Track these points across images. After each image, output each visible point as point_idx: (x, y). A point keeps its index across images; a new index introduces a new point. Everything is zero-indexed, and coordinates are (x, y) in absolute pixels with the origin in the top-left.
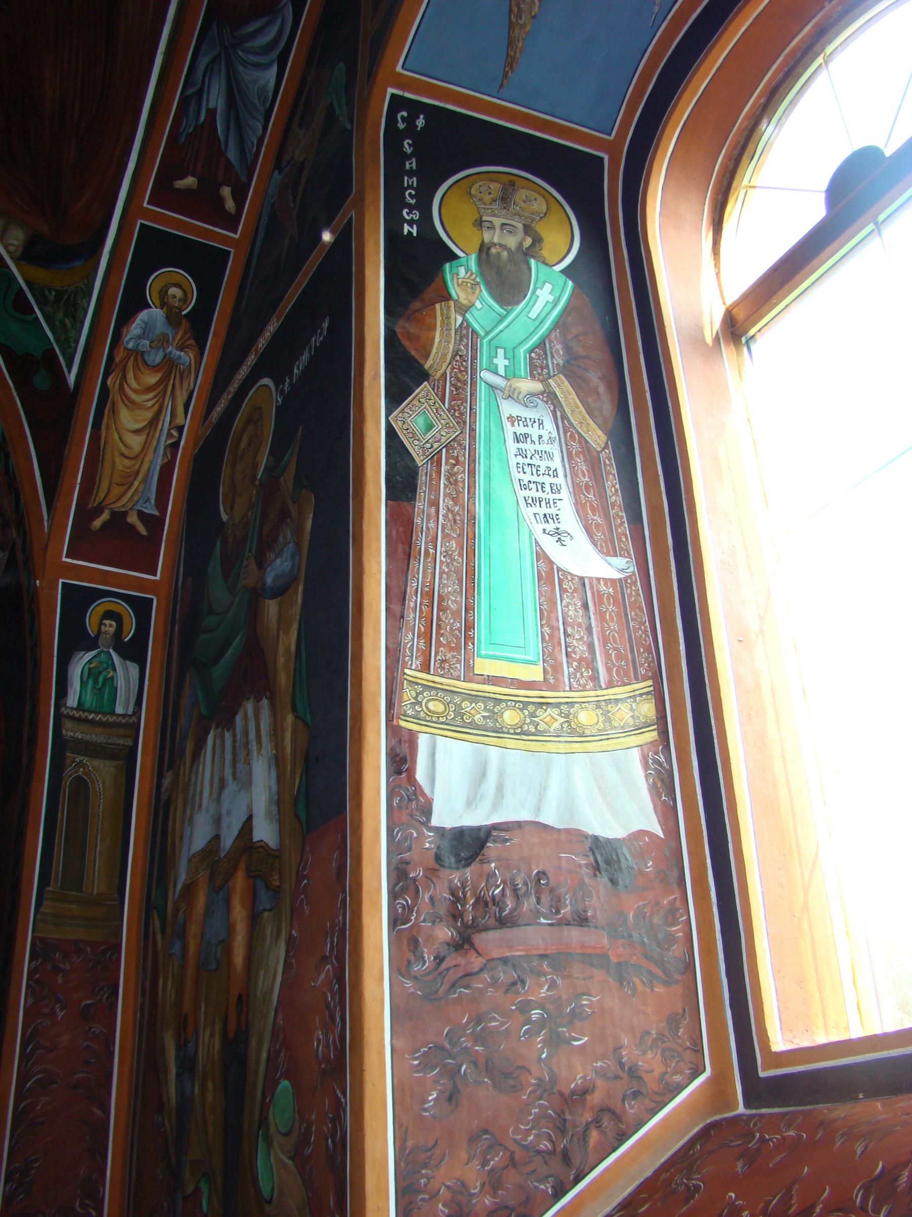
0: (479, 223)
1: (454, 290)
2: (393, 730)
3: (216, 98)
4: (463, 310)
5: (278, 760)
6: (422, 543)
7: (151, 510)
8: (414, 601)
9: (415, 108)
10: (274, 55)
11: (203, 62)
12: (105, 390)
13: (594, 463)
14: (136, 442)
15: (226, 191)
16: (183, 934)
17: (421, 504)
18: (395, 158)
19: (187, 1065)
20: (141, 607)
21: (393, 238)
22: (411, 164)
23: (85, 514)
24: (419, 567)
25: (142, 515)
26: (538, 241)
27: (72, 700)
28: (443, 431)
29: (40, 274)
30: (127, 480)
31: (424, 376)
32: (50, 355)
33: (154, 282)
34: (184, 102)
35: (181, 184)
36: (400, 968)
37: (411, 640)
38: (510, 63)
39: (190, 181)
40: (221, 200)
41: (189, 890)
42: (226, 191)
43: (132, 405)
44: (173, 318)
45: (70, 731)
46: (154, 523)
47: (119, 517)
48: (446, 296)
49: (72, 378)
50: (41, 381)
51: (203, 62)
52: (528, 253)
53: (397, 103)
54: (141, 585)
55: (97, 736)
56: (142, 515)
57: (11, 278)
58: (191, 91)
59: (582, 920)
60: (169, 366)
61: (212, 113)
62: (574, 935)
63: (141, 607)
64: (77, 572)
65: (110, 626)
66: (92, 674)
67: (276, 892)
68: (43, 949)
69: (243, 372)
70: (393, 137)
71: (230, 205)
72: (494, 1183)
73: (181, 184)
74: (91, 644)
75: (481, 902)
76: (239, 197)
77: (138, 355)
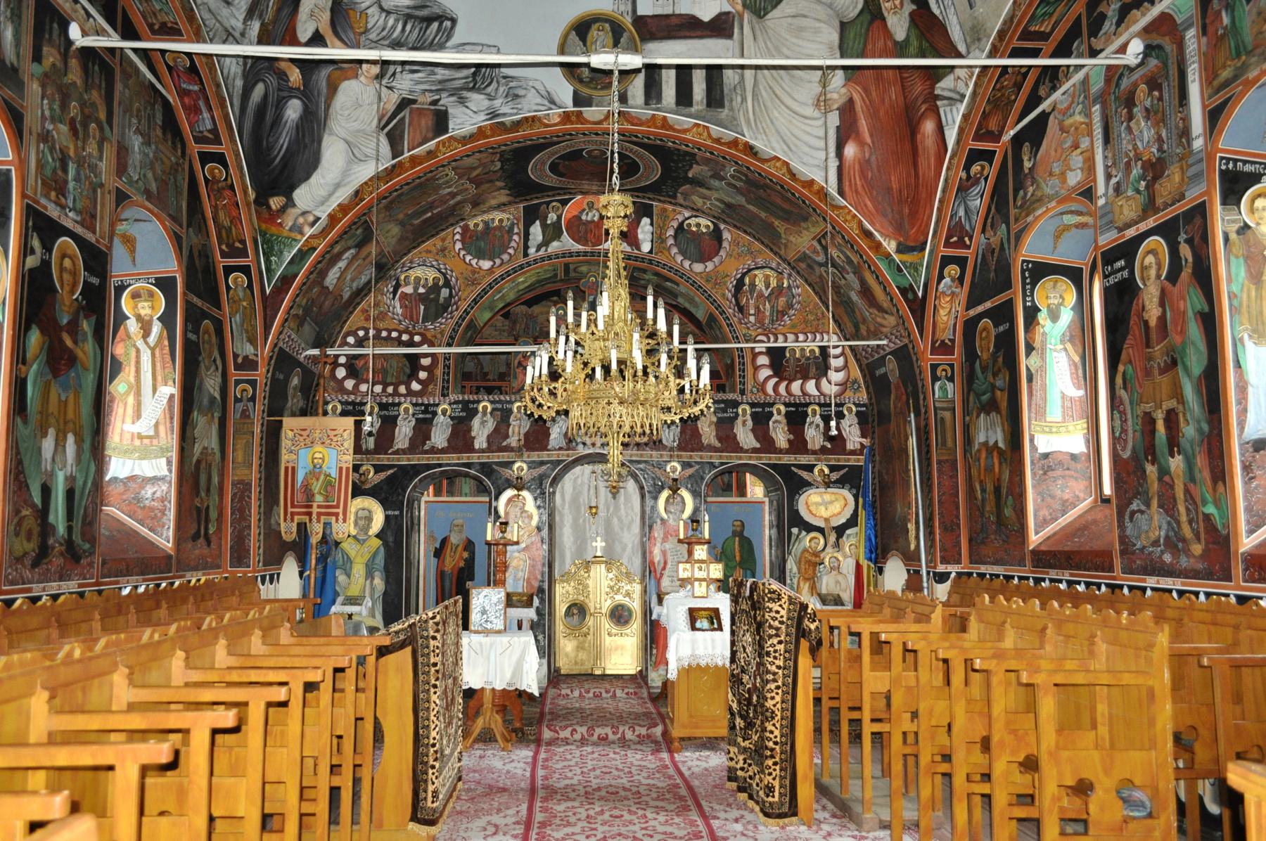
0: (1047, 298)
1: (1041, 321)
2: (1030, 435)
3: (961, 213)
4: (1043, 327)
5: (1003, 430)
6: (1034, 392)
7: (952, 337)
8: (1033, 406)
9: (1028, 262)
12: (935, 306)
13: (1076, 365)
14: (945, 318)
15: (966, 239)
16: (979, 460)
17: (1034, 383)
18: (1024, 278)
19: (983, 491)
20: (952, 366)
21: (1025, 307)
22: (1028, 281)
23: (933, 343)
24: (1034, 398)
25: (949, 340)
26: (1063, 299)
27: (937, 396)
28: (1038, 364)
29: (901, 256)
30: (944, 330)
31: (1034, 349)
32: (911, 285)
33: (946, 271)
34: (952, 216)
35: (952, 240)
36: (1033, 479)
37: (1033, 415)
38: (1055, 248)
39: (955, 239)
41: (979, 451)
42: (966, 239)
43: (943, 308)
44: (953, 280)
45: (937, 405)
46: (953, 341)
47: (943, 341)
48: (1038, 324)
49: (920, 294)
50: (910, 296)
52: (1061, 304)
53: (1024, 261)
54: (951, 360)
55: (945, 405)
56: (949, 340)
57: (894, 260)
59: (1068, 469)
60: (953, 294)
61: (960, 217)
62: (1067, 472)
63: (952, 366)
64: (934, 360)
65: (944, 373)
66: (941, 388)
67: (1005, 459)
68: (939, 462)
69: (980, 309)
70: (1023, 271)
71: (968, 243)
72: (1051, 514)
73: (952, 240)
74: (939, 379)
75: (1049, 467)
76: (971, 238)
77: (943, 293)
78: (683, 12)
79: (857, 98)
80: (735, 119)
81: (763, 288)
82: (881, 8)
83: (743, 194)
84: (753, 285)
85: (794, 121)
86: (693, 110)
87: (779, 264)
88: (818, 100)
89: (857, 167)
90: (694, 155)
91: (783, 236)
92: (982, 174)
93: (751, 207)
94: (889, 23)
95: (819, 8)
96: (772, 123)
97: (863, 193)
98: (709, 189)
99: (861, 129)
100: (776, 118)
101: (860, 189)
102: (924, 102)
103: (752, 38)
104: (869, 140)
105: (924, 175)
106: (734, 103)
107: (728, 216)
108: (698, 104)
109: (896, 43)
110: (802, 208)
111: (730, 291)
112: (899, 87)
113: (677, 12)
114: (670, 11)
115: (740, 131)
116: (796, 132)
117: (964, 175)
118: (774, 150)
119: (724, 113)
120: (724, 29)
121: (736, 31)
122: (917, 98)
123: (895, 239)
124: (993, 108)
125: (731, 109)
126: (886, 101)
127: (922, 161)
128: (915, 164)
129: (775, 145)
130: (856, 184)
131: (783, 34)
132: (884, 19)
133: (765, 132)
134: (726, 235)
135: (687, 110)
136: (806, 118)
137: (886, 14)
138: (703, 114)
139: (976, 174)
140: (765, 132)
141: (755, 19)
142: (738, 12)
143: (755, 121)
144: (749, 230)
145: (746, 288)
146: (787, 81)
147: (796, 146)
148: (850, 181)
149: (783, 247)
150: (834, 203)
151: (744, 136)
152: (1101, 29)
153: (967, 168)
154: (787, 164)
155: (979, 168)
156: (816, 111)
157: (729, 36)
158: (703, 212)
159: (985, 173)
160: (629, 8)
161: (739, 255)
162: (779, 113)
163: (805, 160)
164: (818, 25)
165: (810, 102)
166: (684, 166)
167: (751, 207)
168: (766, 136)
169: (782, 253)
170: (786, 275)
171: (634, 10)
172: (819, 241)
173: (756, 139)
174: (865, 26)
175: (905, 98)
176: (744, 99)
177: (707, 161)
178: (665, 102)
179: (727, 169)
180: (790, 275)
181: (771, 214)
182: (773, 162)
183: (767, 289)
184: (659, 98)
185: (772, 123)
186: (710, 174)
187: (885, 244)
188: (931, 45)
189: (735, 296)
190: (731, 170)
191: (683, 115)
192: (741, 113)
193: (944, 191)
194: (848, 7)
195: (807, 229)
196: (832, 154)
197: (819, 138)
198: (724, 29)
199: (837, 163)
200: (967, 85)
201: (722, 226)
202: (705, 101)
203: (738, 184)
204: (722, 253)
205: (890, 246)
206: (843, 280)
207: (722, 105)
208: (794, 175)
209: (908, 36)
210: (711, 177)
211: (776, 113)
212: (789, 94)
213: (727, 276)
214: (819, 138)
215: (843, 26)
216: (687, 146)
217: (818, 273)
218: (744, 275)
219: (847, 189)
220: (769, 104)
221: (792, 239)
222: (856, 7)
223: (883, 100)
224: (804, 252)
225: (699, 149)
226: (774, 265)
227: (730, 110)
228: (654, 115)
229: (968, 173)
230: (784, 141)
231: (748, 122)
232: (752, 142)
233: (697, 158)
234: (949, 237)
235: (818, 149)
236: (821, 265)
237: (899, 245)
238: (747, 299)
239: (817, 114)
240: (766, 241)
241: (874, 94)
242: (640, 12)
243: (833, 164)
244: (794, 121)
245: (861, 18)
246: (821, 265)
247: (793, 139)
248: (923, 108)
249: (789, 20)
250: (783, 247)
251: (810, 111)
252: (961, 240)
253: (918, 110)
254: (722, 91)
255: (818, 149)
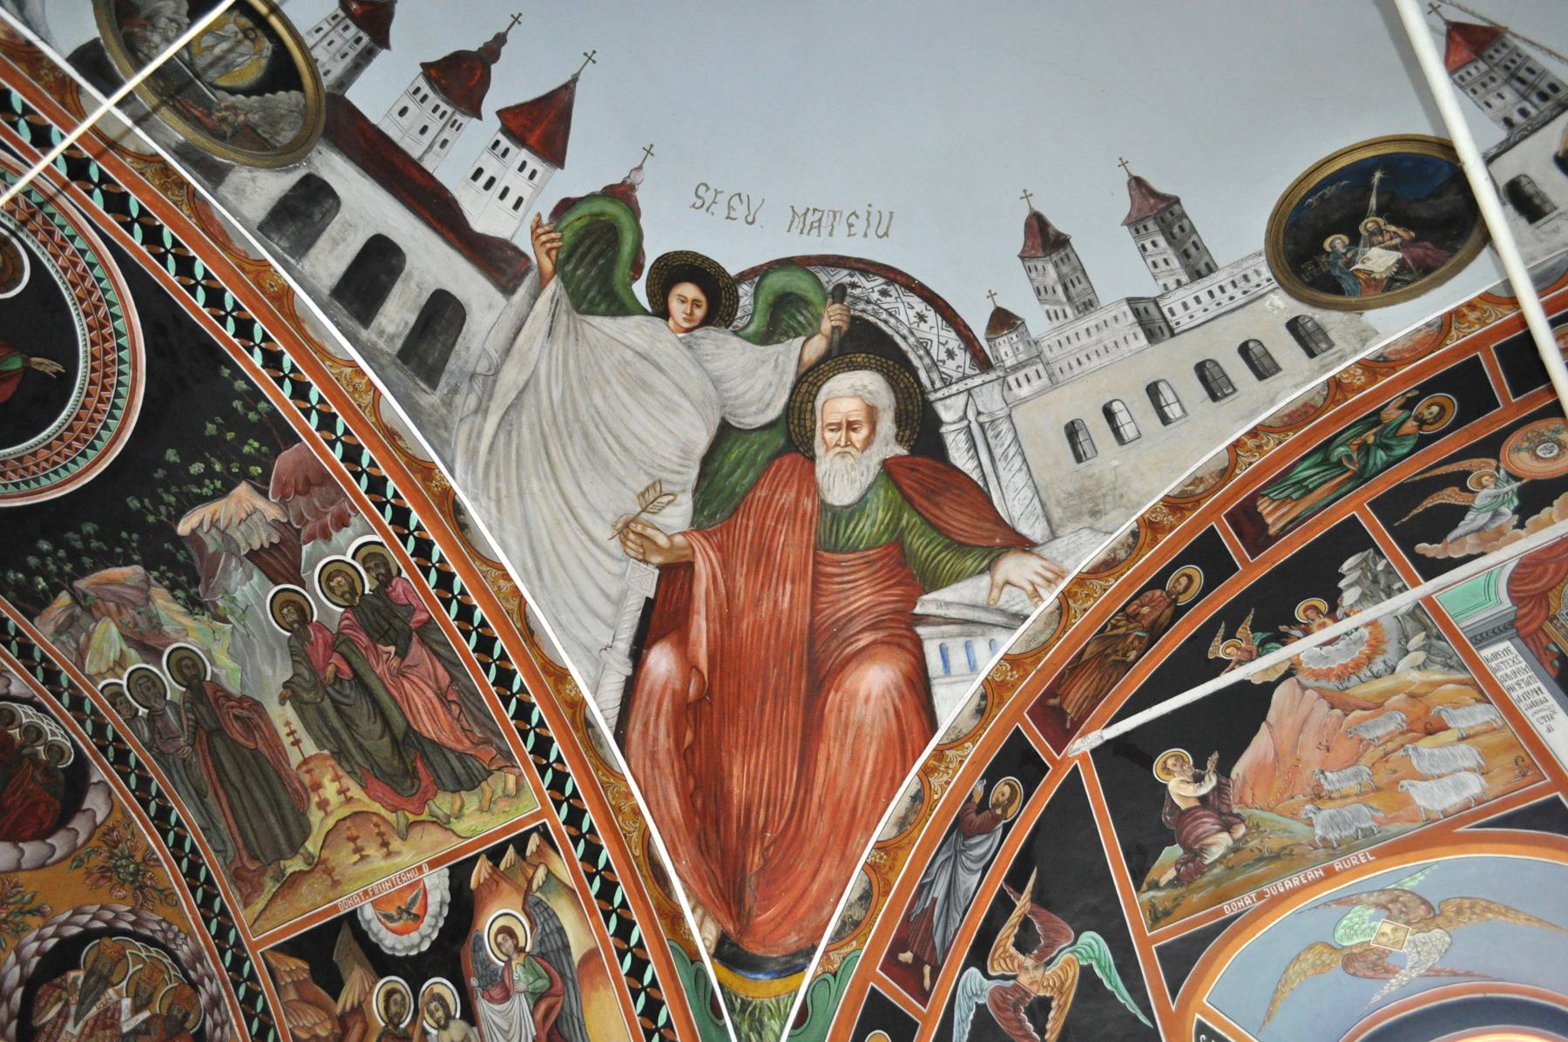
3: (939, 891)
10: (981, 865)
11: (941, 858)
15: (927, 969)
34: (922, 887)
39: (907, 957)
40: (922, 977)
42: (927, 969)
51: (941, 858)
58: (928, 880)
61: (934, 900)
78: (442, 176)
79: (702, 568)
80: (446, 428)
81: (126, 1003)
82: (813, 437)
83: (299, 651)
84: (100, 980)
85: (565, 525)
86: (365, 334)
87: (198, 957)
88: (627, 525)
89: (666, 704)
90: (279, 435)
91: (312, 846)
92: (1004, 815)
93: (283, 716)
94: (821, 468)
95: (693, 372)
96: (521, 493)
97: (668, 770)
98: (194, 605)
99: (693, 634)
100: (532, 494)
101: (662, 756)
102: (873, 627)
103: (545, 328)
104: (703, 663)
105: (830, 784)
106: (458, 400)
107: (158, 741)
108: (381, 333)
109: (824, 507)
110: (491, 735)
111: (21, 961)
112: (805, 588)
113: (428, 165)
114: (415, 153)
115: (448, 459)
116: (561, 548)
117: (978, 787)
118: (506, 551)
119: (430, 399)
120: (503, 272)
121: (522, 292)
122: (850, 618)
123: (717, 921)
124: (1099, 654)
125: (448, 403)
126: (766, 607)
127: (832, 756)
128: (807, 760)
129: (511, 541)
130: (655, 739)
131: (607, 370)
132: (812, 459)
133: (499, 501)
134: (95, 802)
135: (353, 324)
136: (593, 540)
137: (819, 450)
138: (384, 361)
139: (996, 806)
140: (499, 501)
141: (565, 302)
142: (540, 266)
143: (488, 464)
144: (183, 811)
145: (77, 976)
146: (578, 449)
147: (552, 573)
148: (646, 725)
149: (271, 887)
150: (598, 749)
151: (452, 472)
152: (1455, 526)
153: (992, 777)
154: (522, 602)
155: (1007, 789)
156: (616, 541)
157: (508, 290)
158: (77, 704)
159: (1012, 811)
160: (338, 69)
161: (105, 872)
162: (542, 490)
163: (563, 618)
164: (677, 397)
165: (610, 517)
166: (210, 473)
167: (283, 716)
168: (499, 509)
169: (243, 916)
170: (203, 999)
171: (344, 82)
172: (459, 874)
173: (475, 499)
174: (768, 453)
175: (815, 612)
176: (481, 409)
177: (314, 480)
178: (306, 266)
179: (339, 538)
180: (215, 1001)
181: (341, 755)
182: (494, 572)
183: (136, 1010)
184: (302, 245)
185: (521, 493)
186: (262, 537)
187: (691, 920)
188: (926, 521)
189: (31, 985)
190: (347, 544)
191: (337, 324)
192: (465, 428)
193: (903, 823)
194: (750, 405)
195: (442, 823)
196: (624, 645)
197: (607, 596)
198: (503, 272)
199: (628, 671)
200: (1035, 595)
201: (98, 774)
202: (399, 343)
203: (327, 610)
204: (80, 824)
205: (702, 934)
206: (457, 1028)
207: (433, 383)
208: (532, 633)
209: (863, 499)
210: (253, 555)
211: (535, 485)
212: (573, 472)
213: (38, 911)
214: (607, 596)
215: (725, 433)
216: (301, 391)
217: (348, 997)
218: (88, 935)
219: (635, 736)
220: (528, 457)
221: (343, 857)
222: (762, 411)
223: (757, 603)
224: (352, 916)
225: (327, 422)
226: (184, 952)
227: (444, 403)
228: (264, 263)
229: (988, 790)
230: (533, 550)
231: (472, 454)
232: (462, 497)
233: (285, 460)
234: (899, 945)
235: (596, 615)
236: (382, 963)
237: (722, 940)
238: (63, 1015)
239: (614, 546)
240: (211, 863)
241: (741, 581)
242: (353, 95)
243: (619, 669)
244: (565, 525)
245: (765, 436)
246: (382, 963)
247: (553, 559)
248: (866, 639)
249: (629, 355)
250: (271, 887)
251: (603, 533)
252: (918, 962)
253: (848, 641)
254: (444, 359)
255: (596, 615)
